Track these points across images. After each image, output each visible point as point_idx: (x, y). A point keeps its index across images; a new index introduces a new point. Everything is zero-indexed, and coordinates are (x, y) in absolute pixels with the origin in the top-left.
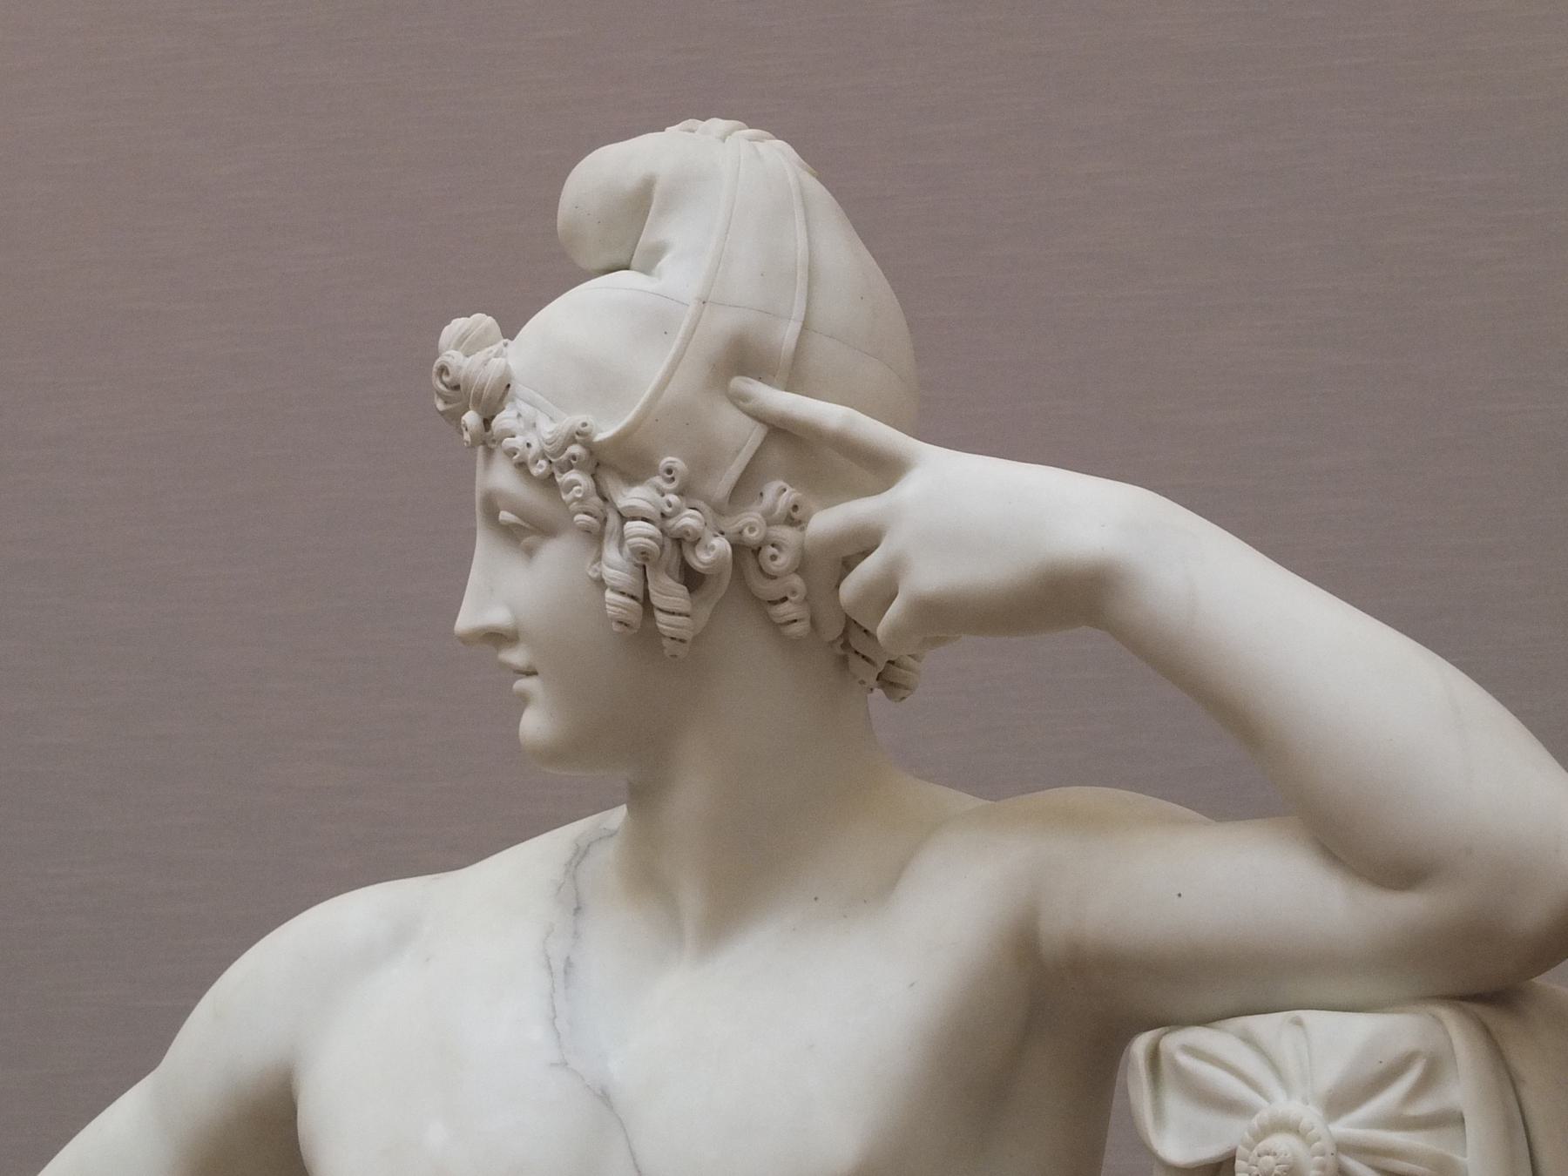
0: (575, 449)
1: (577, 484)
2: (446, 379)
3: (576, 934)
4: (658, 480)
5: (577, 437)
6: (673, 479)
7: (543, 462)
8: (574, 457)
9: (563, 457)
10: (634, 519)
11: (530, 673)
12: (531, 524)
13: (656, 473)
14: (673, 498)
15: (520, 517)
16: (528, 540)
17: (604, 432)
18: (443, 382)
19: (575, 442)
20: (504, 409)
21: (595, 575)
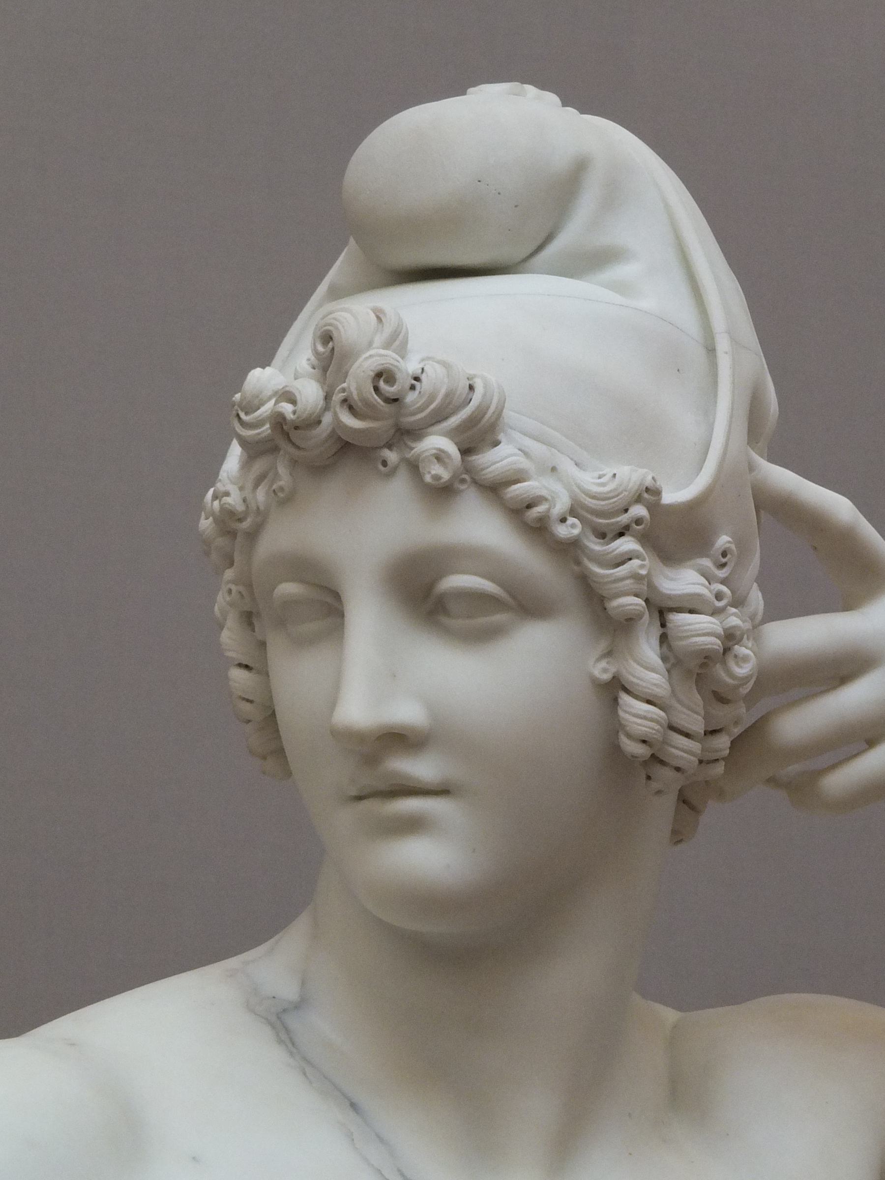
0: (639, 511)
1: (627, 558)
2: (382, 384)
3: (381, 1139)
4: (706, 563)
5: (646, 495)
6: (724, 565)
7: (571, 520)
8: (638, 521)
9: (624, 519)
10: (679, 610)
11: (441, 791)
12: (514, 597)
13: (707, 556)
14: (724, 588)
15: (500, 584)
16: (499, 618)
17: (670, 497)
18: (376, 389)
19: (638, 500)
20: (496, 443)
21: (606, 677)
